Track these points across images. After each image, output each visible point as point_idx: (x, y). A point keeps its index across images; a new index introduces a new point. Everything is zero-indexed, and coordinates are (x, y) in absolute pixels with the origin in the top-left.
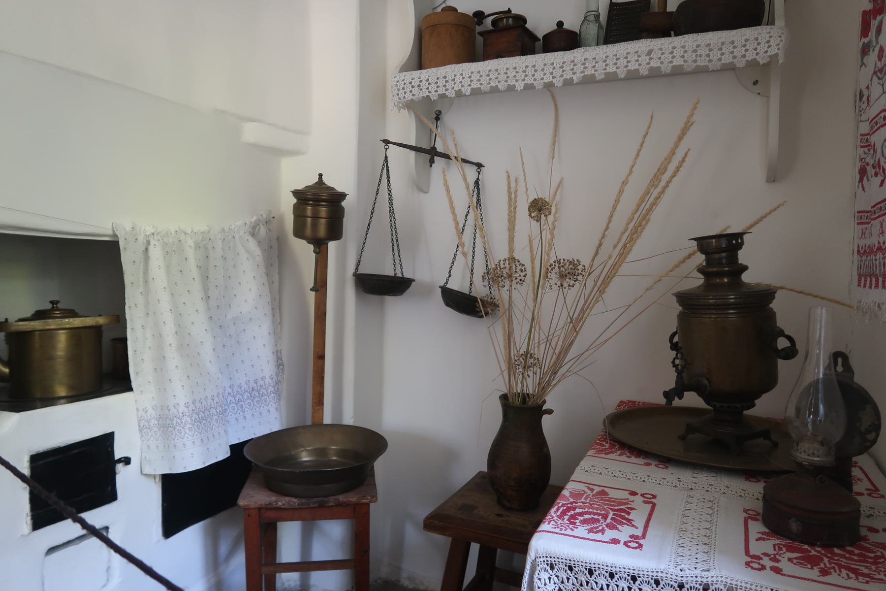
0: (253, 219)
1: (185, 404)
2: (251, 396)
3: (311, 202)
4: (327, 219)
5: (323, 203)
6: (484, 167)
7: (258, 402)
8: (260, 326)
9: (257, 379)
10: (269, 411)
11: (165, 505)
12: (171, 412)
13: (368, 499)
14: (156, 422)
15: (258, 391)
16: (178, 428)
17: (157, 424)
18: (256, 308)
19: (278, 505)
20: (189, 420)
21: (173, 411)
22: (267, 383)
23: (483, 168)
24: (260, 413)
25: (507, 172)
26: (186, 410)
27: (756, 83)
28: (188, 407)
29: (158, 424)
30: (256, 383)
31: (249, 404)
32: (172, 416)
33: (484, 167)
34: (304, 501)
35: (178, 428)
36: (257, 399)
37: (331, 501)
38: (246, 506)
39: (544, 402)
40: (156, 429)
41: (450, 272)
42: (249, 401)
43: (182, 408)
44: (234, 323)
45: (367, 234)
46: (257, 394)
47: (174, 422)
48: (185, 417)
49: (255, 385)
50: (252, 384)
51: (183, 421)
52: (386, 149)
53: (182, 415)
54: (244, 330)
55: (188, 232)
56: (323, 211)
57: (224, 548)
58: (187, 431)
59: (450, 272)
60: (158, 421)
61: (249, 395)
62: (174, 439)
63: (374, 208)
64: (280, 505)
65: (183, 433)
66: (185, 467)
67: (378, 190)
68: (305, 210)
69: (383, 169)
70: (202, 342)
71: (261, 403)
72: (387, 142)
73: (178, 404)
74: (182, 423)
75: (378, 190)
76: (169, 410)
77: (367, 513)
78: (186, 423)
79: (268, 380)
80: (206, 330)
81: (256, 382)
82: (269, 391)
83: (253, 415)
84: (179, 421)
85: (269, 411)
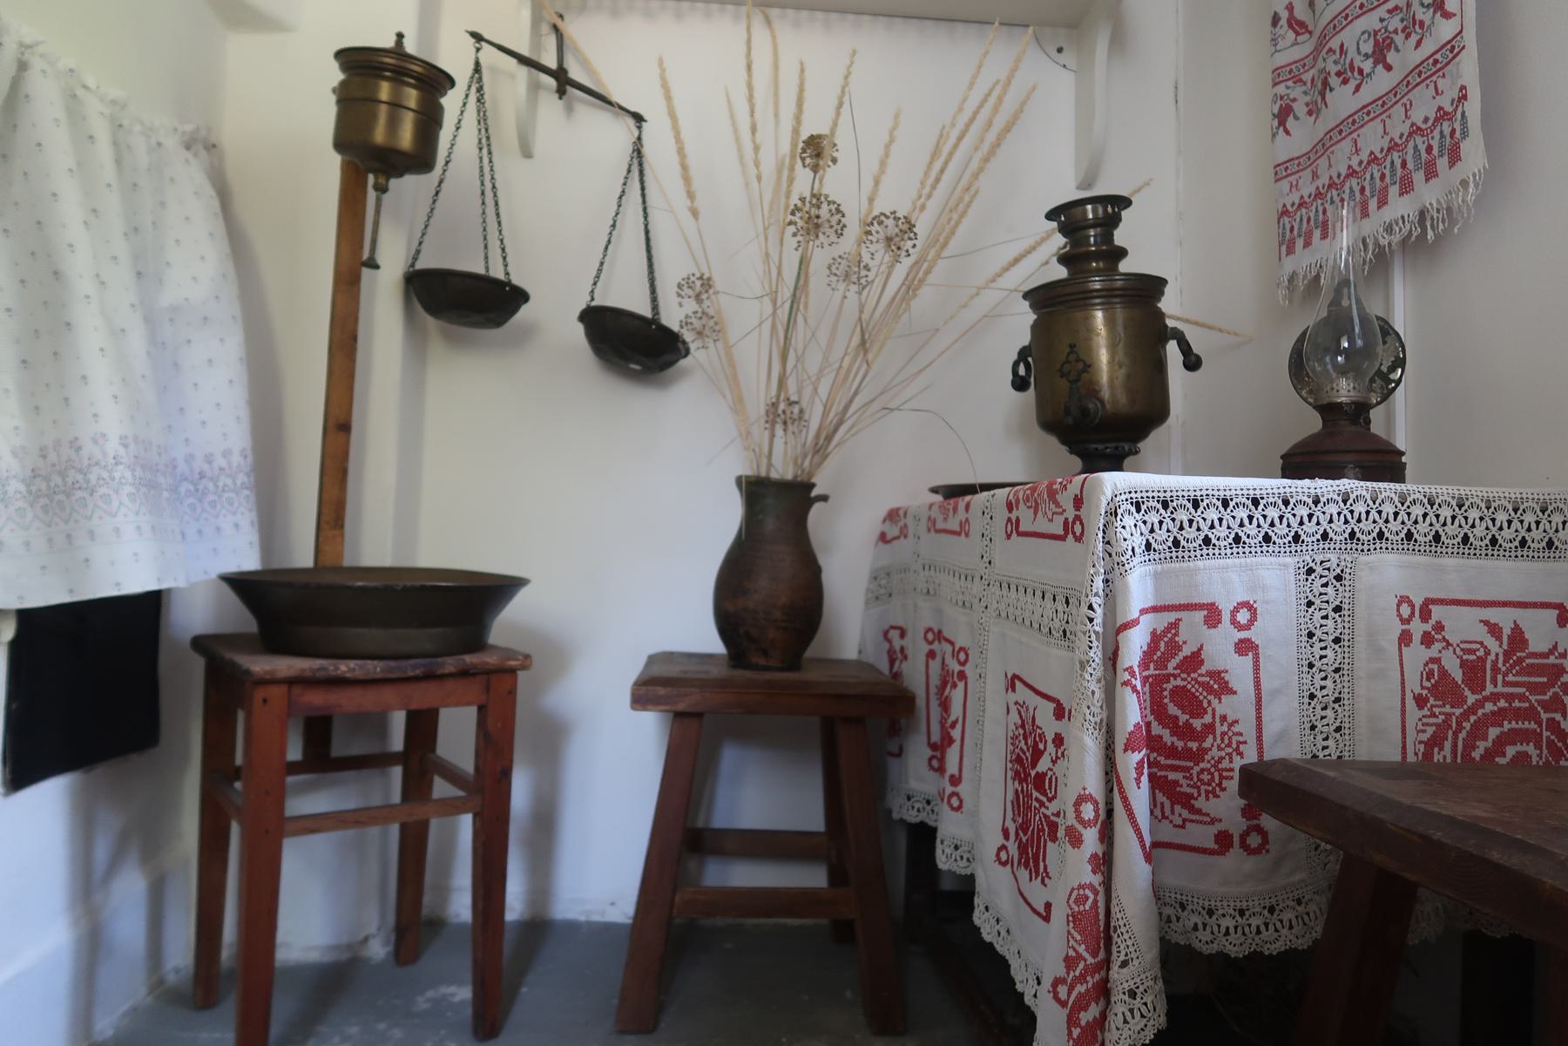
0: (189, 128)
1: (121, 438)
2: (197, 490)
3: (387, 74)
4: (424, 117)
5: (412, 81)
6: (645, 121)
7: (213, 504)
8: (222, 340)
9: (212, 455)
10: (237, 526)
11: (14, 706)
12: (85, 453)
13: (519, 660)
14: (22, 488)
15: (214, 480)
16: (103, 490)
17: (25, 492)
18: (217, 297)
19: (339, 672)
20: (128, 474)
21: (88, 448)
22: (235, 464)
23: (643, 123)
24: (218, 529)
25: (802, 64)
26: (122, 451)
27: (1060, 50)
28: (126, 446)
29: (30, 492)
30: (210, 462)
31: (193, 508)
32: (86, 462)
33: (645, 121)
34: (392, 663)
35: (103, 490)
36: (211, 497)
37: (450, 664)
38: (267, 672)
39: (813, 486)
40: (20, 504)
41: (592, 292)
42: (191, 500)
43: (113, 446)
44: (171, 320)
45: (434, 201)
46: (211, 486)
47: (93, 477)
48: (121, 467)
49: (206, 467)
50: (199, 464)
51: (117, 475)
52: (478, 50)
53: (113, 462)
54: (189, 341)
55: (90, 85)
56: (412, 97)
57: (102, 852)
58: (126, 500)
59: (592, 292)
60: (28, 486)
61: (192, 488)
62: (90, 518)
63: (450, 153)
64: (345, 672)
65: (115, 504)
66: (118, 584)
67: (460, 121)
68: (376, 89)
69: (469, 87)
70: (123, 330)
71: (219, 507)
72: (477, 37)
73: (104, 435)
74: (113, 479)
75: (460, 121)
76: (79, 449)
77: (512, 692)
78: (123, 481)
79: (236, 459)
80: (133, 306)
81: (209, 459)
82: (239, 482)
83: (200, 532)
84: (105, 475)
85: (237, 526)
